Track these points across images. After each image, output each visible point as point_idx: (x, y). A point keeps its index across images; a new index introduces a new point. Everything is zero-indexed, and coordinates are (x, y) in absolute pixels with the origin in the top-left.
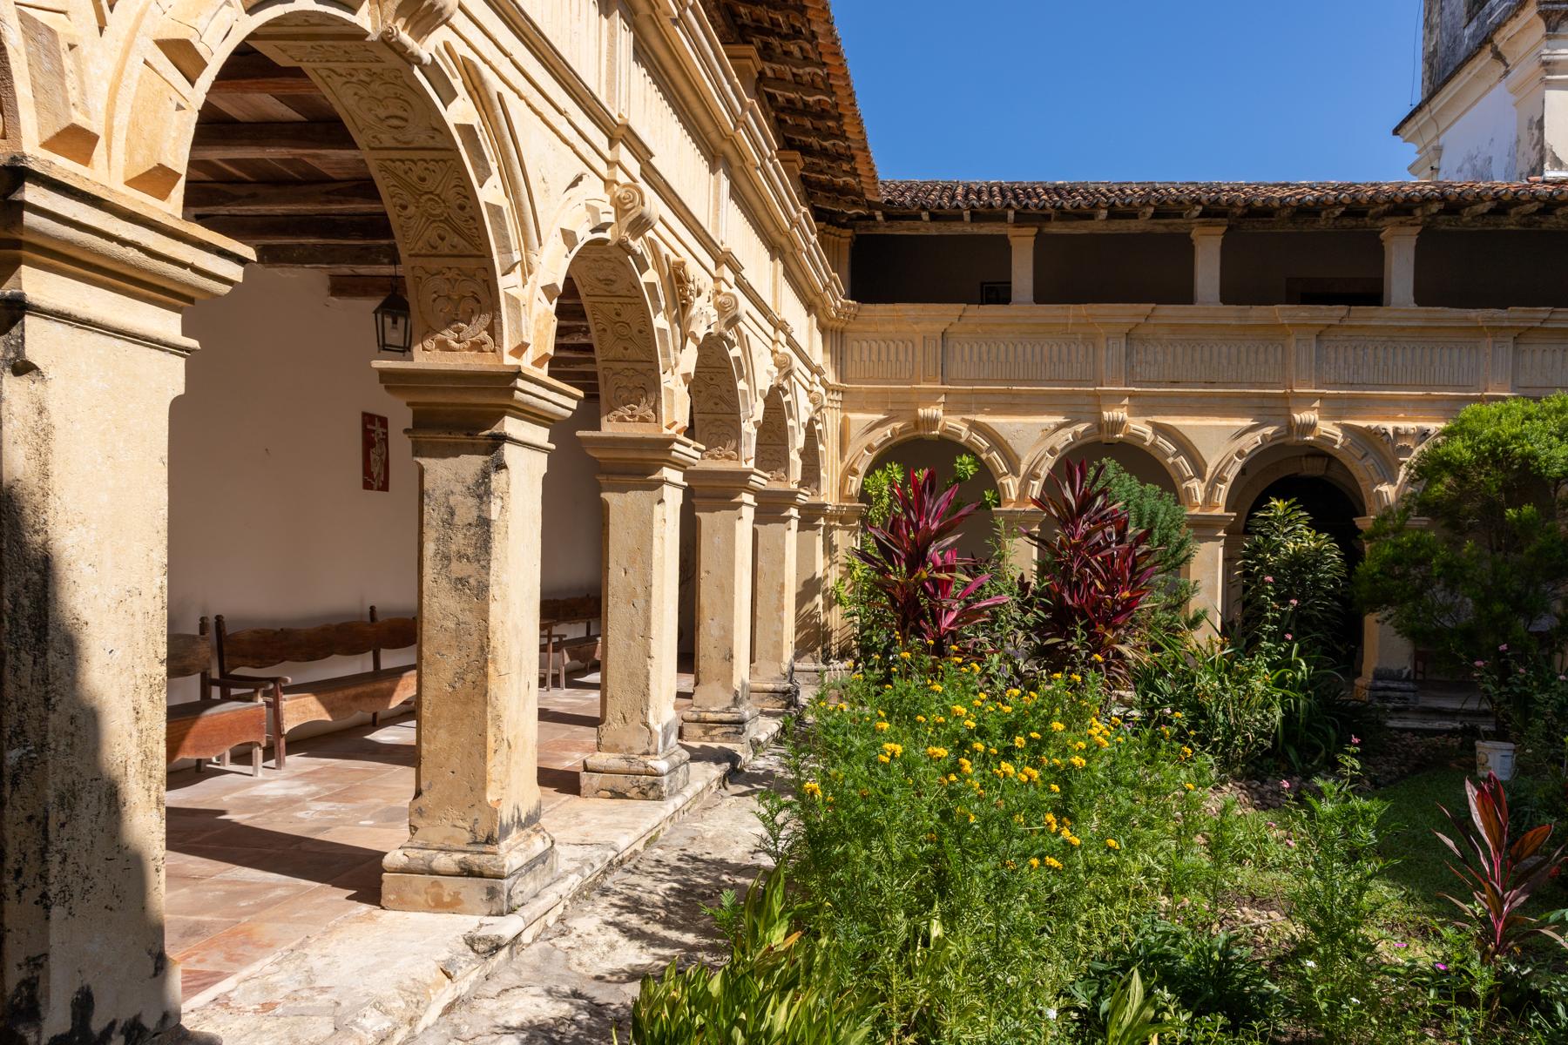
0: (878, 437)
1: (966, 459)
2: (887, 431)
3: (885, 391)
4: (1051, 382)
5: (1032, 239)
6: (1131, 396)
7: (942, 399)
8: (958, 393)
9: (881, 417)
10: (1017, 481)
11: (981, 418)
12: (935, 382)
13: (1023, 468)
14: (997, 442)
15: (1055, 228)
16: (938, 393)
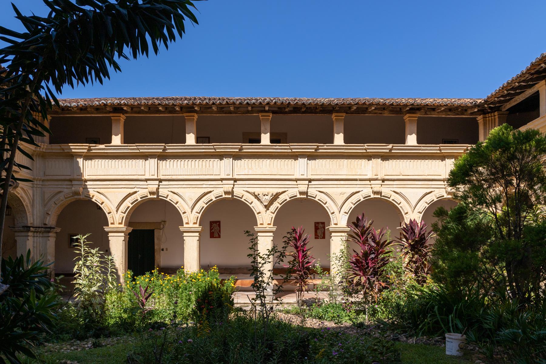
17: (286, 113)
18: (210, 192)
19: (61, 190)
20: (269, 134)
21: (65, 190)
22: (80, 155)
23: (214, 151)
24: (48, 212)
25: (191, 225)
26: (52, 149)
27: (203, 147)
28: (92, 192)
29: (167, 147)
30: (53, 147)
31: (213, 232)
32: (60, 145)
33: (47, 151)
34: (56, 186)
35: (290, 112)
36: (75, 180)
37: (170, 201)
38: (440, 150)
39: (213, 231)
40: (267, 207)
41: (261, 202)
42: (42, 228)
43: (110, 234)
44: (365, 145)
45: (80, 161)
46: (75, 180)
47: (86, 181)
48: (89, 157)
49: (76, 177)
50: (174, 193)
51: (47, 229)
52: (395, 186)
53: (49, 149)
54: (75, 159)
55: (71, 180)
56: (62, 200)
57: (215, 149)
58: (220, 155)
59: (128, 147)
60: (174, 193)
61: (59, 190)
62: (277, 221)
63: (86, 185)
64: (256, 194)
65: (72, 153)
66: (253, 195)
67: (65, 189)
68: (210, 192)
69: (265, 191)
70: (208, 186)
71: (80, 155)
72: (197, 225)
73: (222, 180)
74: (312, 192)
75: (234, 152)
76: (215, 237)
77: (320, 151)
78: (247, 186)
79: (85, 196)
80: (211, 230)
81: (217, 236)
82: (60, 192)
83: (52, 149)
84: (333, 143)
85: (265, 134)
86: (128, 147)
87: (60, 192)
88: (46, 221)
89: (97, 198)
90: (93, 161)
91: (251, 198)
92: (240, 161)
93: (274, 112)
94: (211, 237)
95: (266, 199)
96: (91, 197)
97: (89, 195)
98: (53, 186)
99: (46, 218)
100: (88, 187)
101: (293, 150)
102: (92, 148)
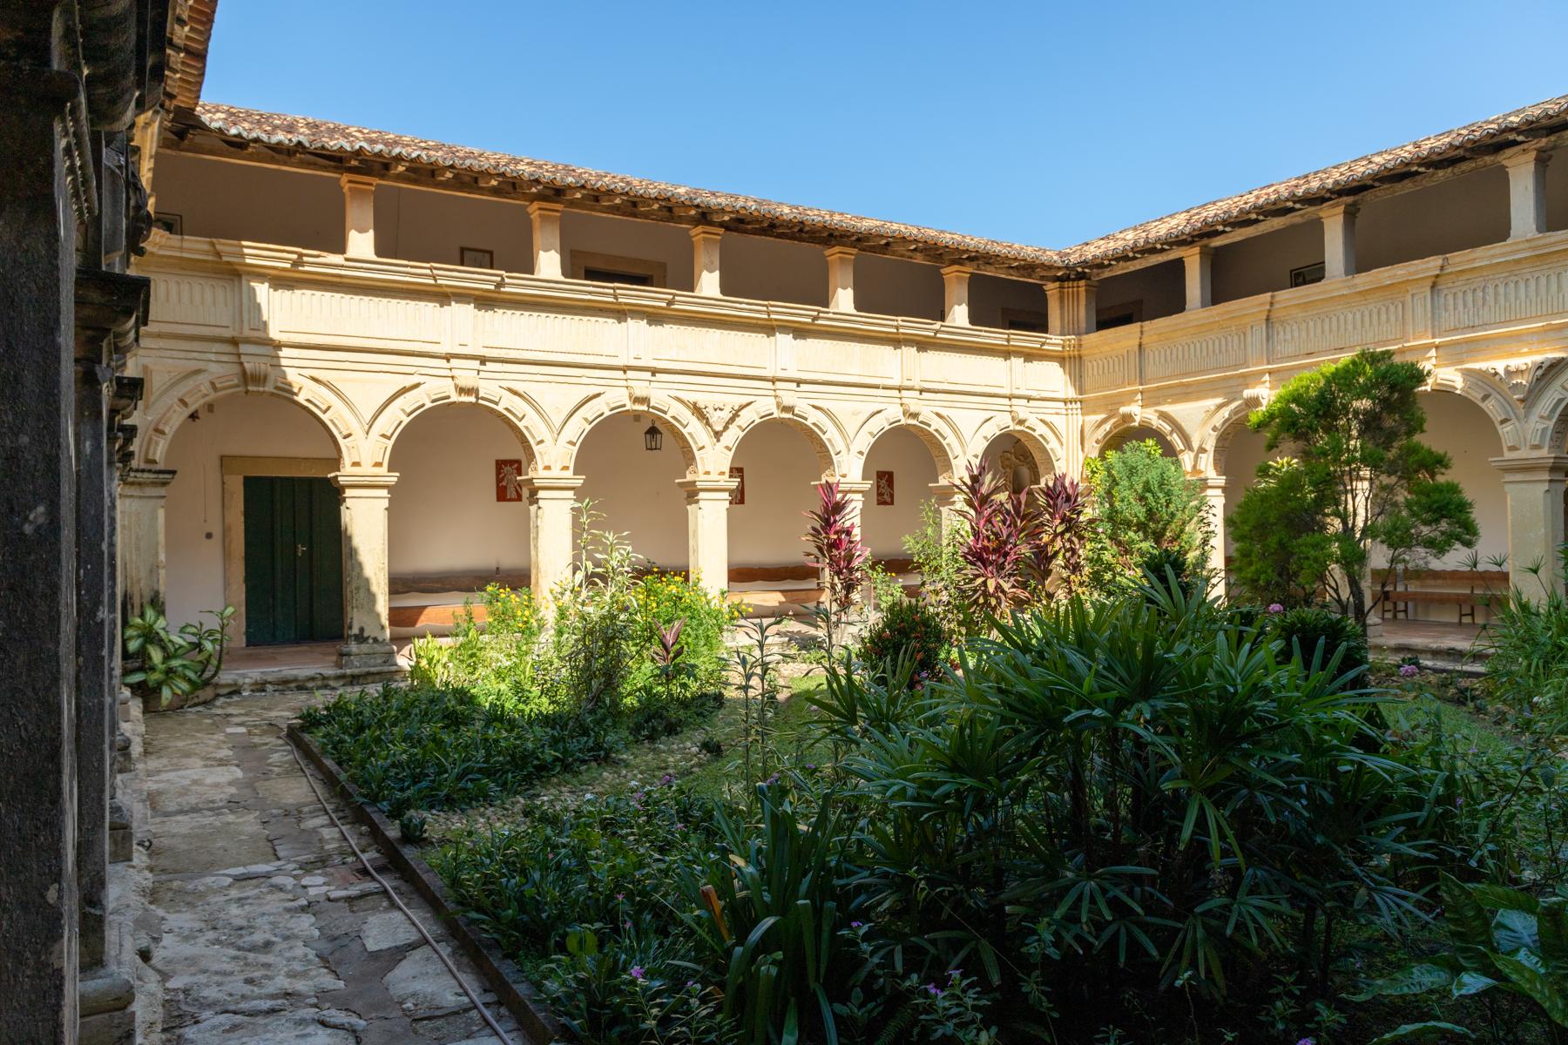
0: (1100, 433)
1: (1150, 442)
2: (1107, 427)
3: (1105, 397)
4: (1215, 370)
5: (1198, 257)
6: (1270, 373)
7: (1139, 396)
8: (1149, 390)
9: (1103, 416)
10: (1192, 455)
11: (1165, 408)
12: (1134, 384)
13: (1195, 445)
14: (1177, 427)
15: (1217, 242)
16: (1135, 393)
17: (746, 232)
18: (598, 395)
19: (201, 365)
20: (717, 273)
21: (213, 368)
22: (261, 275)
23: (612, 300)
24: (161, 427)
25: (556, 472)
26: (181, 249)
27: (591, 289)
28: (292, 376)
29: (507, 280)
30: (185, 245)
31: (505, 487)
32: (214, 240)
33: (162, 252)
34: (182, 355)
35: (755, 232)
36: (248, 341)
37: (505, 413)
38: (1008, 340)
39: (504, 483)
40: (718, 435)
41: (708, 423)
42: (143, 471)
43: (348, 493)
44: (900, 318)
45: (262, 290)
46: (248, 341)
47: (279, 346)
48: (282, 281)
49: (247, 333)
50: (515, 393)
51: (161, 476)
52: (938, 403)
53: (172, 248)
54: (244, 282)
55: (234, 342)
56: (206, 395)
57: (616, 297)
58: (618, 311)
59: (409, 269)
60: (515, 393)
61: (194, 365)
62: (583, 462)
63: (278, 357)
64: (701, 405)
65: (239, 268)
66: (688, 407)
67: (213, 365)
68: (598, 395)
69: (719, 400)
70: (594, 381)
71: (261, 275)
72: (570, 473)
73: (625, 369)
74: (802, 407)
75: (654, 307)
76: (510, 500)
77: (820, 322)
78: (676, 386)
79: (277, 388)
80: (499, 481)
81: (514, 495)
82: (198, 372)
83: (181, 249)
84: (827, 306)
85: (711, 272)
86: (409, 269)
87: (198, 372)
88: (154, 454)
89: (307, 393)
90: (298, 292)
91: (686, 415)
92: (659, 327)
93: (726, 226)
94: (499, 499)
95: (718, 418)
96: (296, 390)
97: (290, 385)
98: (176, 354)
99: (157, 443)
100: (283, 362)
101: (773, 316)
102: (305, 259)
